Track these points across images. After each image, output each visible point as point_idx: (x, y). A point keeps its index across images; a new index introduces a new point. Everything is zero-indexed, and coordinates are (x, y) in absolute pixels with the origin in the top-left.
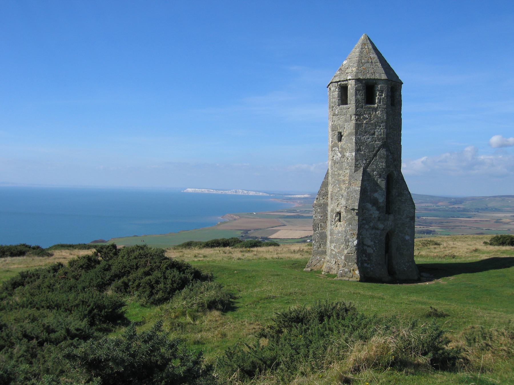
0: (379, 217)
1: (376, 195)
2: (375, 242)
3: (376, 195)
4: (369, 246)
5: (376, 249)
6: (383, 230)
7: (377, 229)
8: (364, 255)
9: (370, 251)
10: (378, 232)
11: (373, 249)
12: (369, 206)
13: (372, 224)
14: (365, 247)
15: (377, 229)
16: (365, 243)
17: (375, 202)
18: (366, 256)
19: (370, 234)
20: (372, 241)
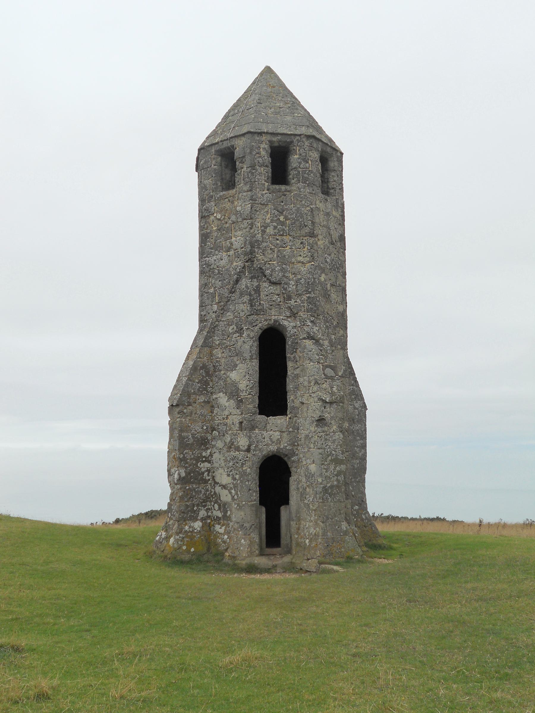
0: (241, 423)
1: (234, 375)
2: (234, 479)
3: (234, 375)
4: (224, 487)
5: (237, 494)
6: (248, 450)
7: (238, 449)
8: (216, 506)
9: (225, 496)
10: (240, 455)
11: (231, 493)
12: (223, 399)
13: (228, 439)
14: (218, 489)
15: (238, 449)
16: (217, 480)
17: (233, 393)
18: (219, 509)
19: (226, 460)
20: (228, 475)
